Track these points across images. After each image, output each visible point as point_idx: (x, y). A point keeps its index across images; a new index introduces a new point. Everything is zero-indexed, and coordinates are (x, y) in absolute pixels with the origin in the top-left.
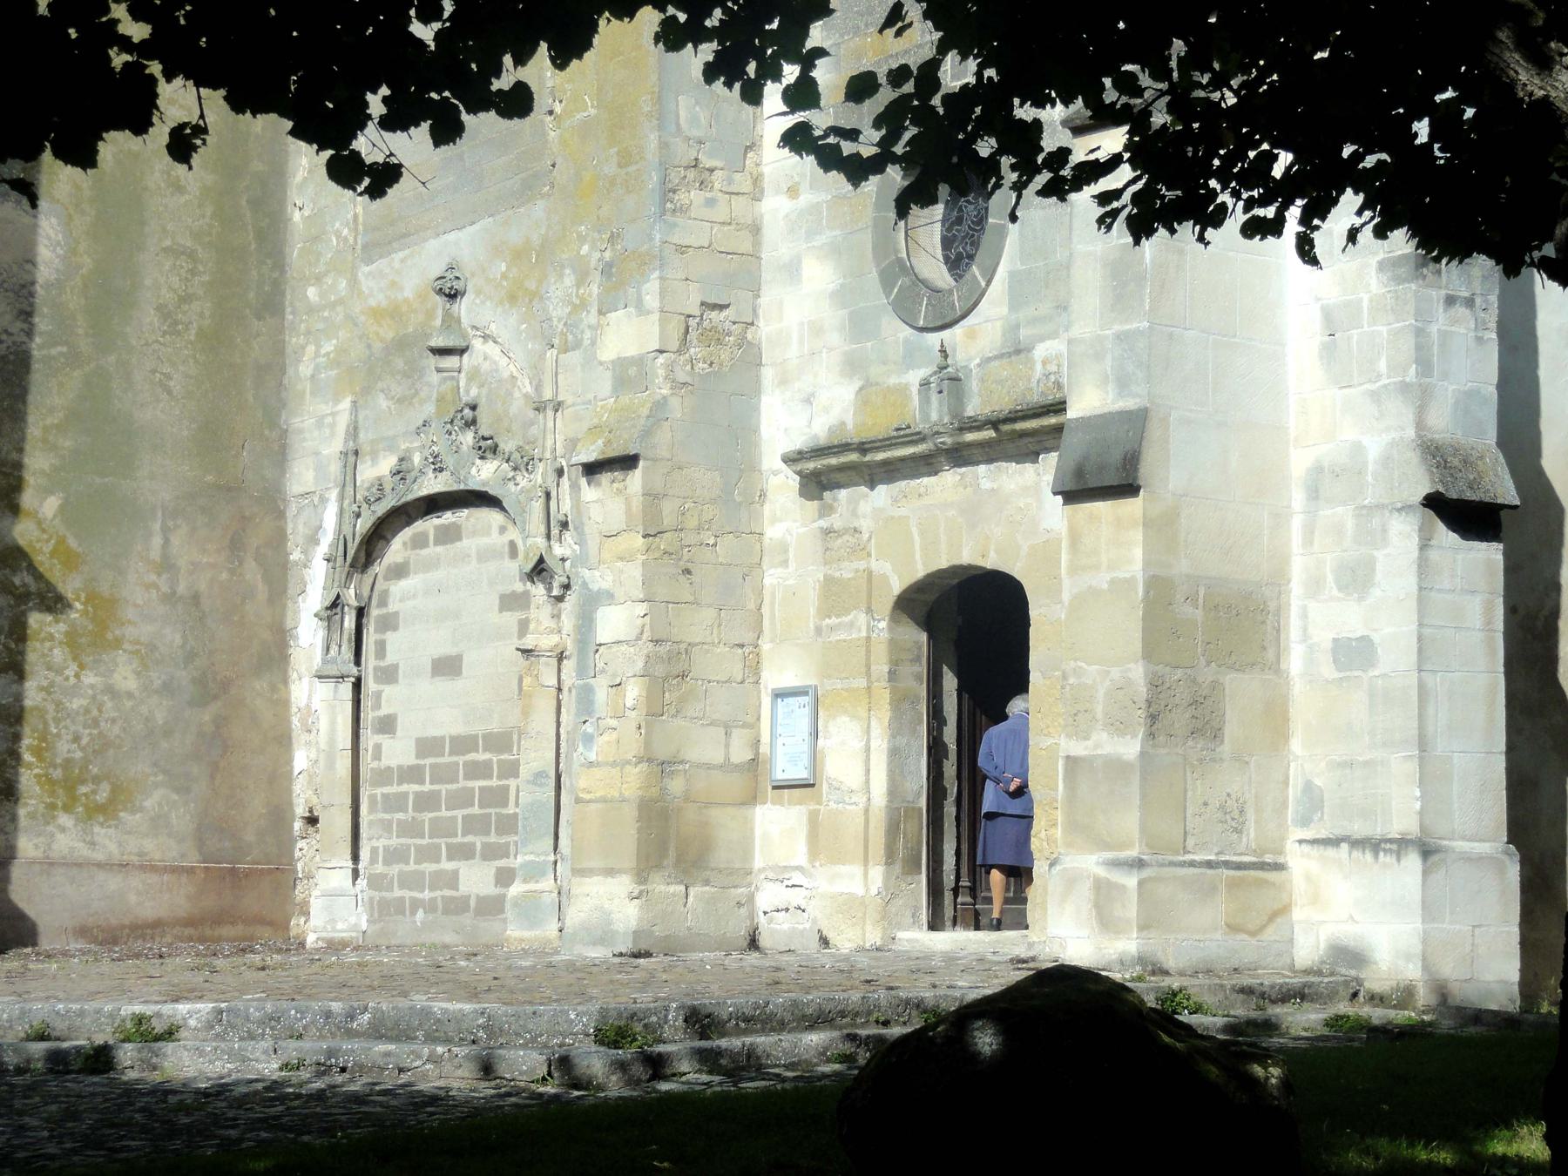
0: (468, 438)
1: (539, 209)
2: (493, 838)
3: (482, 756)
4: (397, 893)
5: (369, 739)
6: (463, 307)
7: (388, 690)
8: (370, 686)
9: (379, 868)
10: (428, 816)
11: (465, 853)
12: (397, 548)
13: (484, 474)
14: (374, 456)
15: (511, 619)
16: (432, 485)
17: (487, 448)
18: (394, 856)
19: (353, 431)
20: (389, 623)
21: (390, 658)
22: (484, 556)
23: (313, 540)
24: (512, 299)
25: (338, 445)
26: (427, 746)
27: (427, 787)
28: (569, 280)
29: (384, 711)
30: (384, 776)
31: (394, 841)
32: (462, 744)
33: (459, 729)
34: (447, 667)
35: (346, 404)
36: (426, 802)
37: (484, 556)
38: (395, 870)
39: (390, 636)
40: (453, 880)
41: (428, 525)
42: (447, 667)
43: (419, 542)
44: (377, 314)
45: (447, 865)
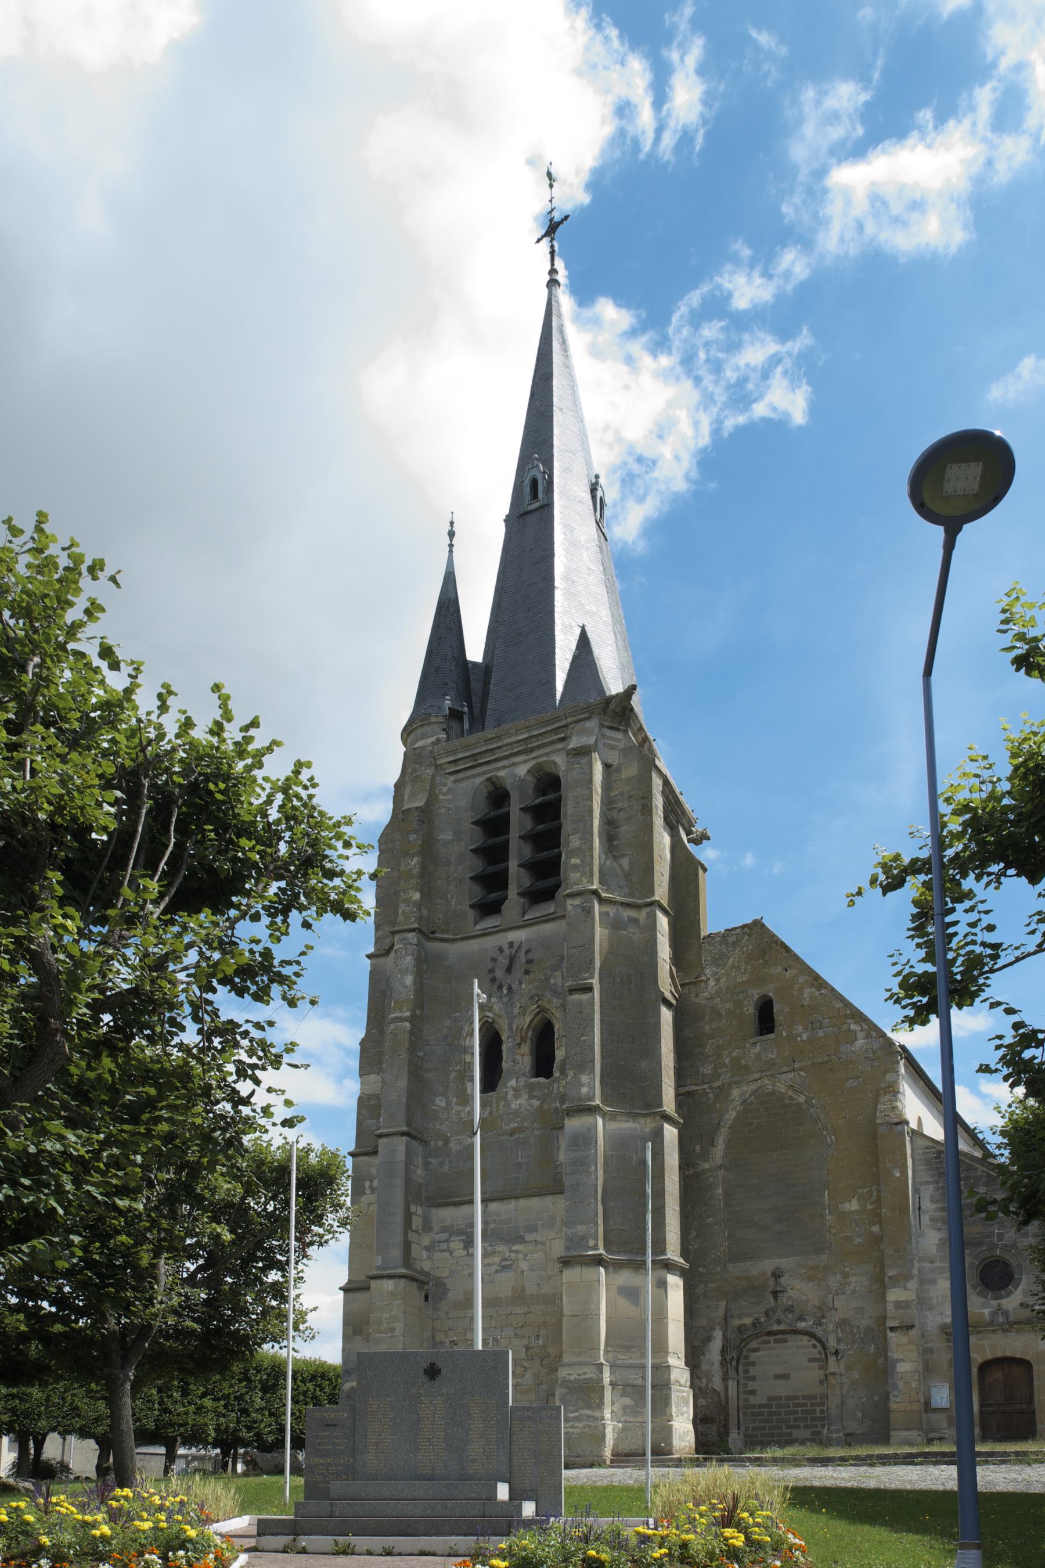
0: (790, 1316)
1: (824, 1257)
2: (809, 1423)
3: (801, 1401)
4: (760, 1438)
5: (742, 1397)
6: (782, 1280)
7: (750, 1383)
8: (742, 1381)
9: (750, 1432)
10: (774, 1418)
11: (798, 1427)
12: (754, 1344)
13: (802, 1325)
14: (740, 1317)
15: (816, 1365)
16: (776, 1327)
17: (801, 1318)
18: (754, 1429)
19: (727, 1311)
20: (753, 1364)
21: (751, 1374)
22: (798, 1348)
23: (709, 1339)
24: (810, 1279)
25: (721, 1313)
26: (770, 1398)
27: (774, 1409)
28: (839, 1277)
29: (749, 1388)
30: (753, 1406)
31: (757, 1424)
32: (788, 1398)
33: (791, 1394)
34: (785, 1377)
35: (724, 1302)
36: (770, 1414)
37: (798, 1348)
38: (759, 1433)
39: (751, 1368)
40: (790, 1434)
41: (772, 1338)
42: (785, 1377)
43: (768, 1342)
44: (738, 1278)
45: (784, 1430)
